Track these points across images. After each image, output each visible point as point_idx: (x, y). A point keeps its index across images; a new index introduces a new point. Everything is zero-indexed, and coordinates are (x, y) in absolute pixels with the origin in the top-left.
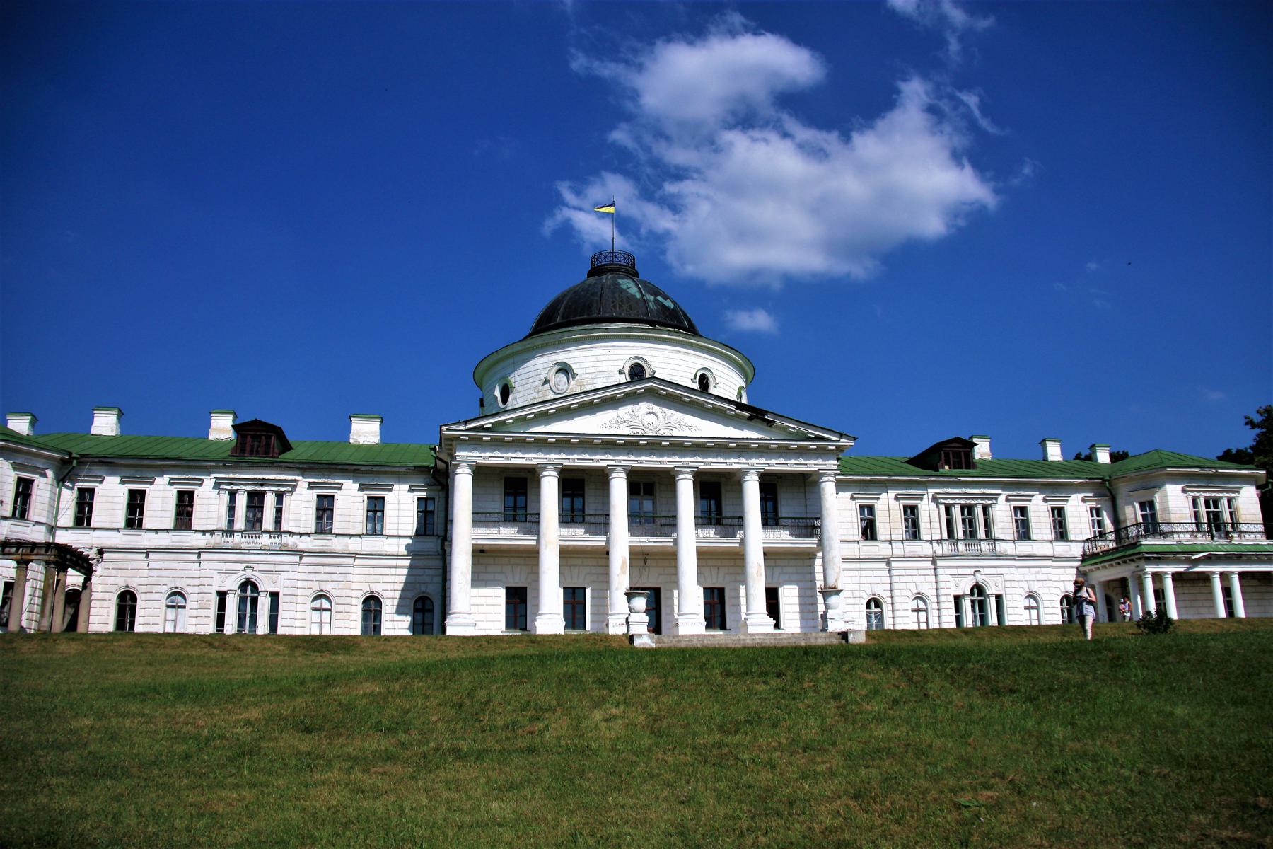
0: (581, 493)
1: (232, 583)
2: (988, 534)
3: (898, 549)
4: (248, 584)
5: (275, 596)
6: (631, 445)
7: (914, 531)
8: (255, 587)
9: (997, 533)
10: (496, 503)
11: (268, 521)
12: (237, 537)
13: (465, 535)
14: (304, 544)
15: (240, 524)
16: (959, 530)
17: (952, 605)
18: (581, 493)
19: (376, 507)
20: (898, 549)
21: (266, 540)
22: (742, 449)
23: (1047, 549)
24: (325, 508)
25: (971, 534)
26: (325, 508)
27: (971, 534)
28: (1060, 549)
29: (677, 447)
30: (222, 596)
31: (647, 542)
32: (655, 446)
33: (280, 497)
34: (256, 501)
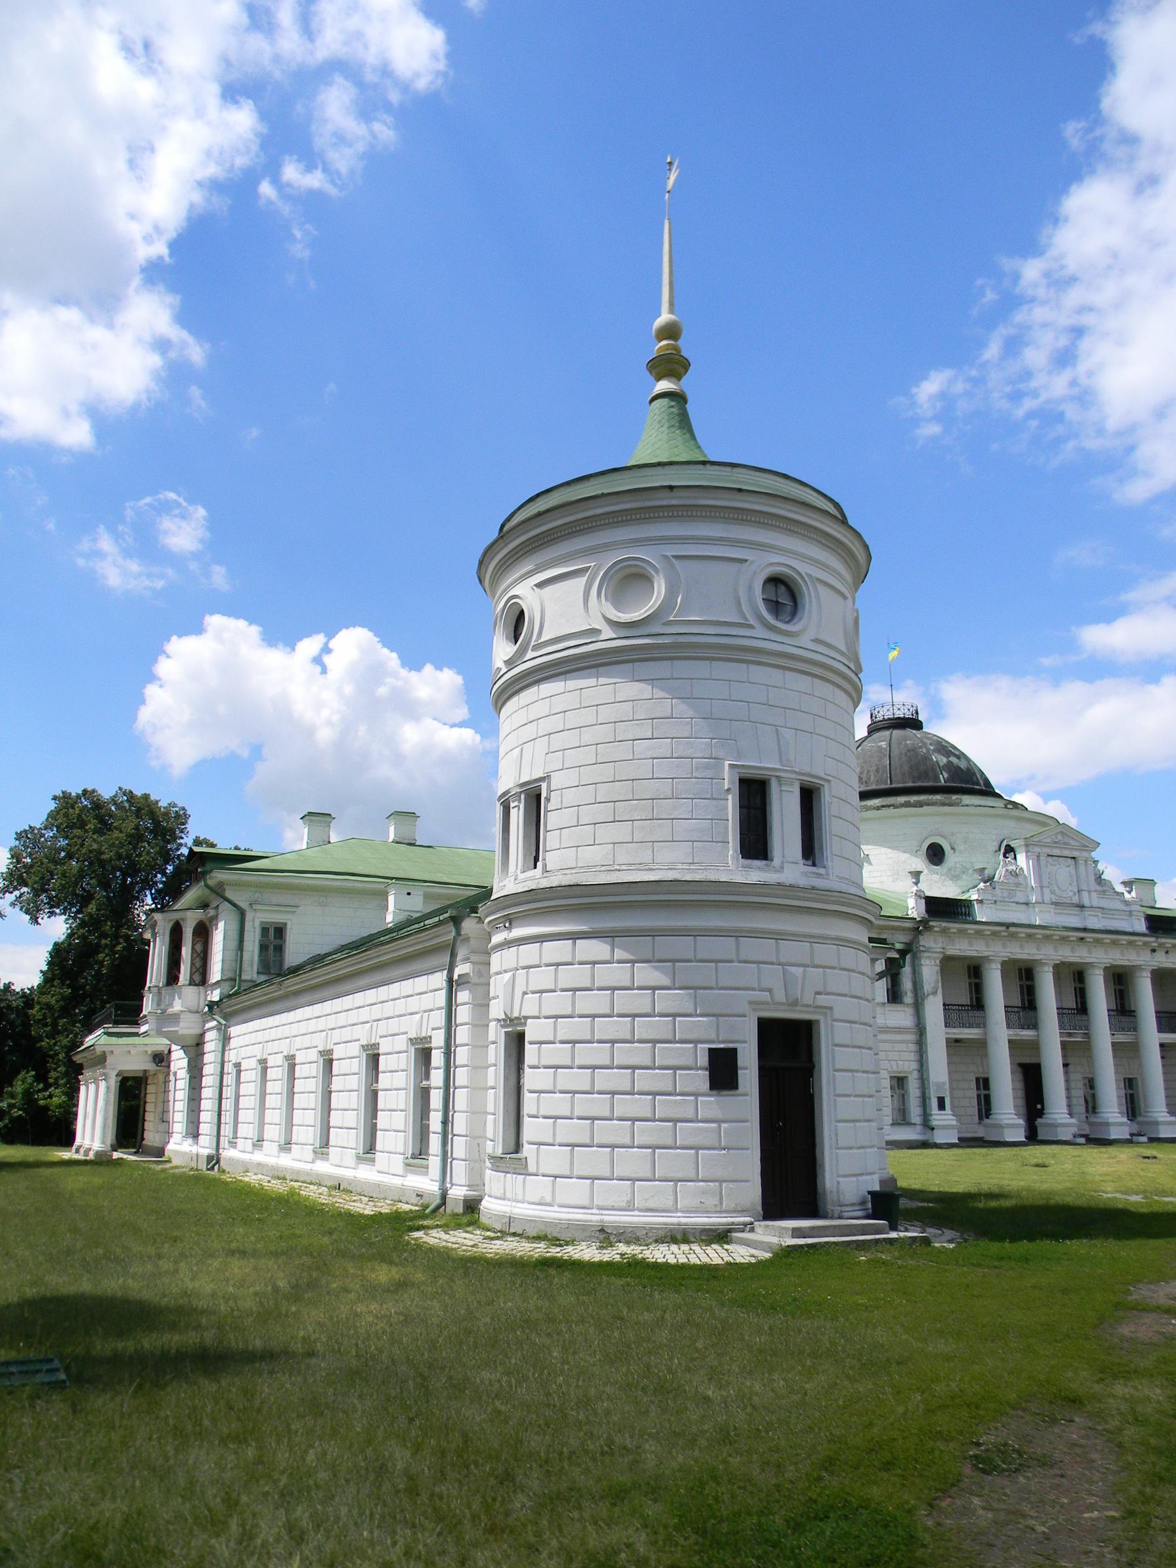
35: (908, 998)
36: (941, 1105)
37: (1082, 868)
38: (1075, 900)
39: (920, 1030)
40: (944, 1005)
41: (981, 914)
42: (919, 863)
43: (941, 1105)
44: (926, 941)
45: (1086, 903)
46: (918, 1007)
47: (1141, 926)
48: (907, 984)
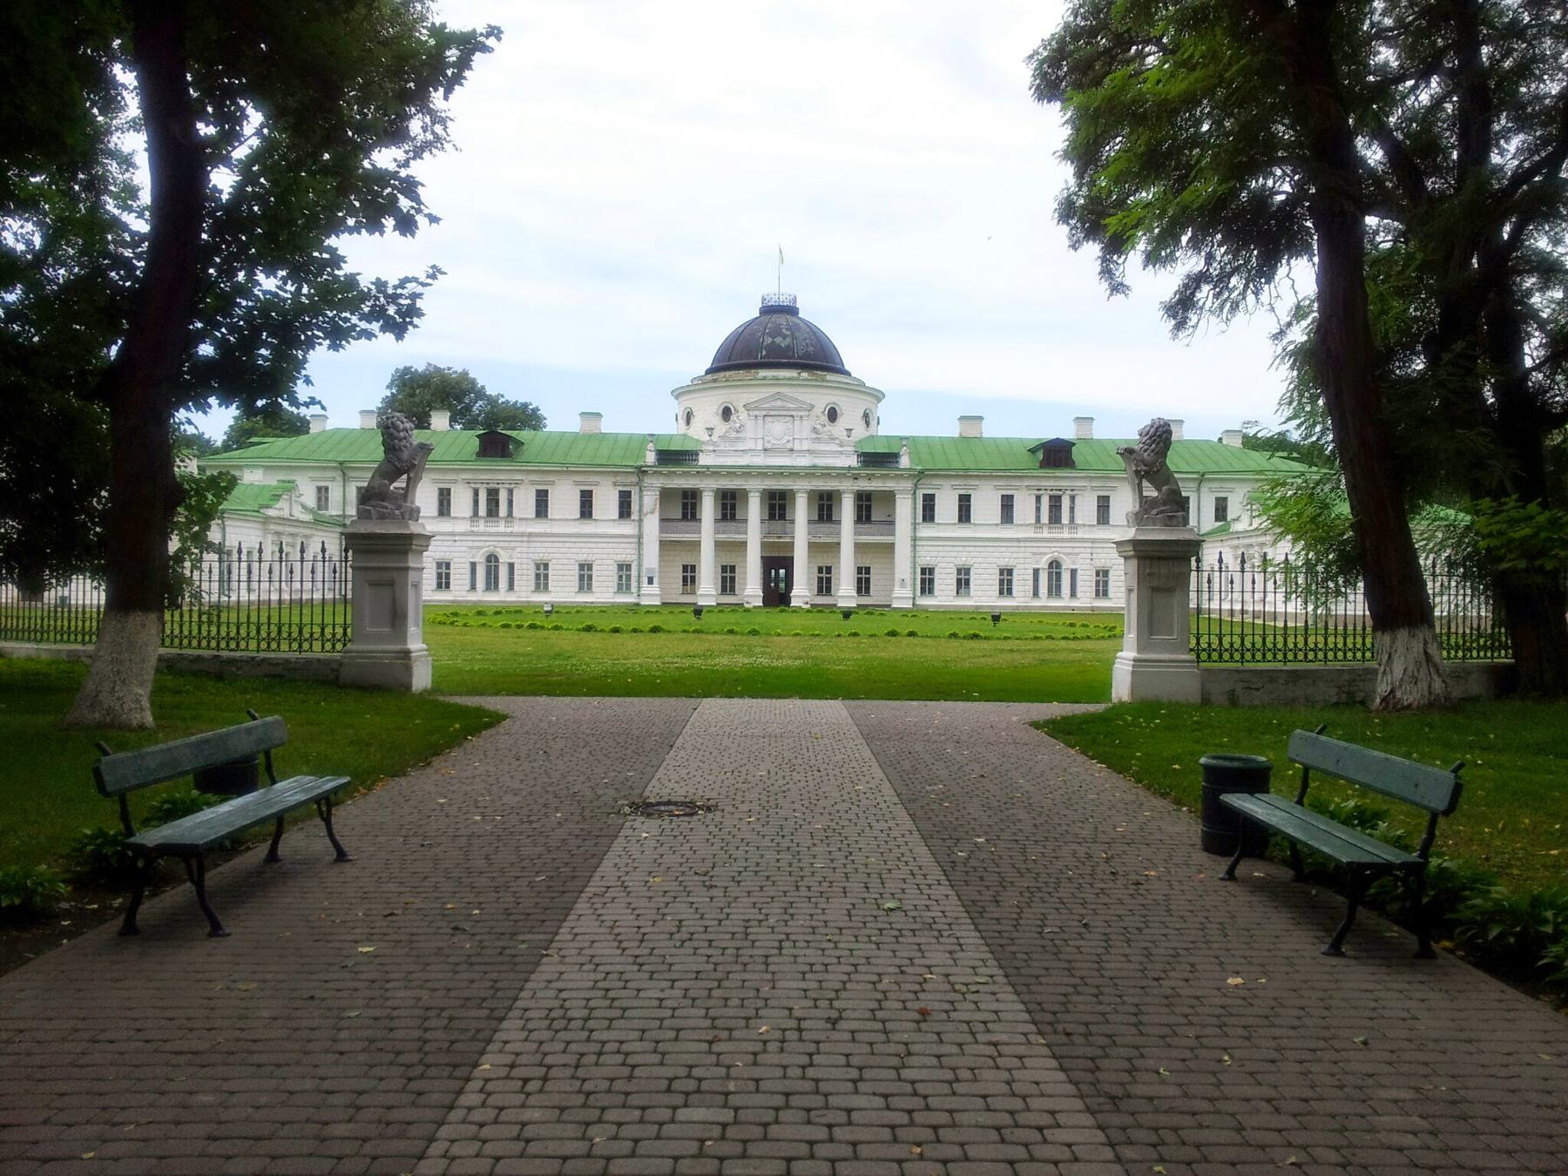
2: (1072, 519)
5: (511, 566)
8: (497, 560)
9: (1078, 521)
11: (503, 510)
12: (482, 522)
15: (482, 511)
16: (1045, 519)
17: (1031, 577)
21: (502, 523)
25: (1055, 518)
27: (1055, 518)
30: (473, 565)
33: (511, 492)
34: (493, 496)
35: (635, 516)
36: (650, 581)
37: (797, 422)
38: (789, 446)
39: (640, 537)
40: (662, 520)
41: (704, 460)
42: (716, 421)
43: (650, 581)
44: (648, 481)
45: (797, 447)
46: (641, 521)
47: (853, 461)
48: (635, 507)
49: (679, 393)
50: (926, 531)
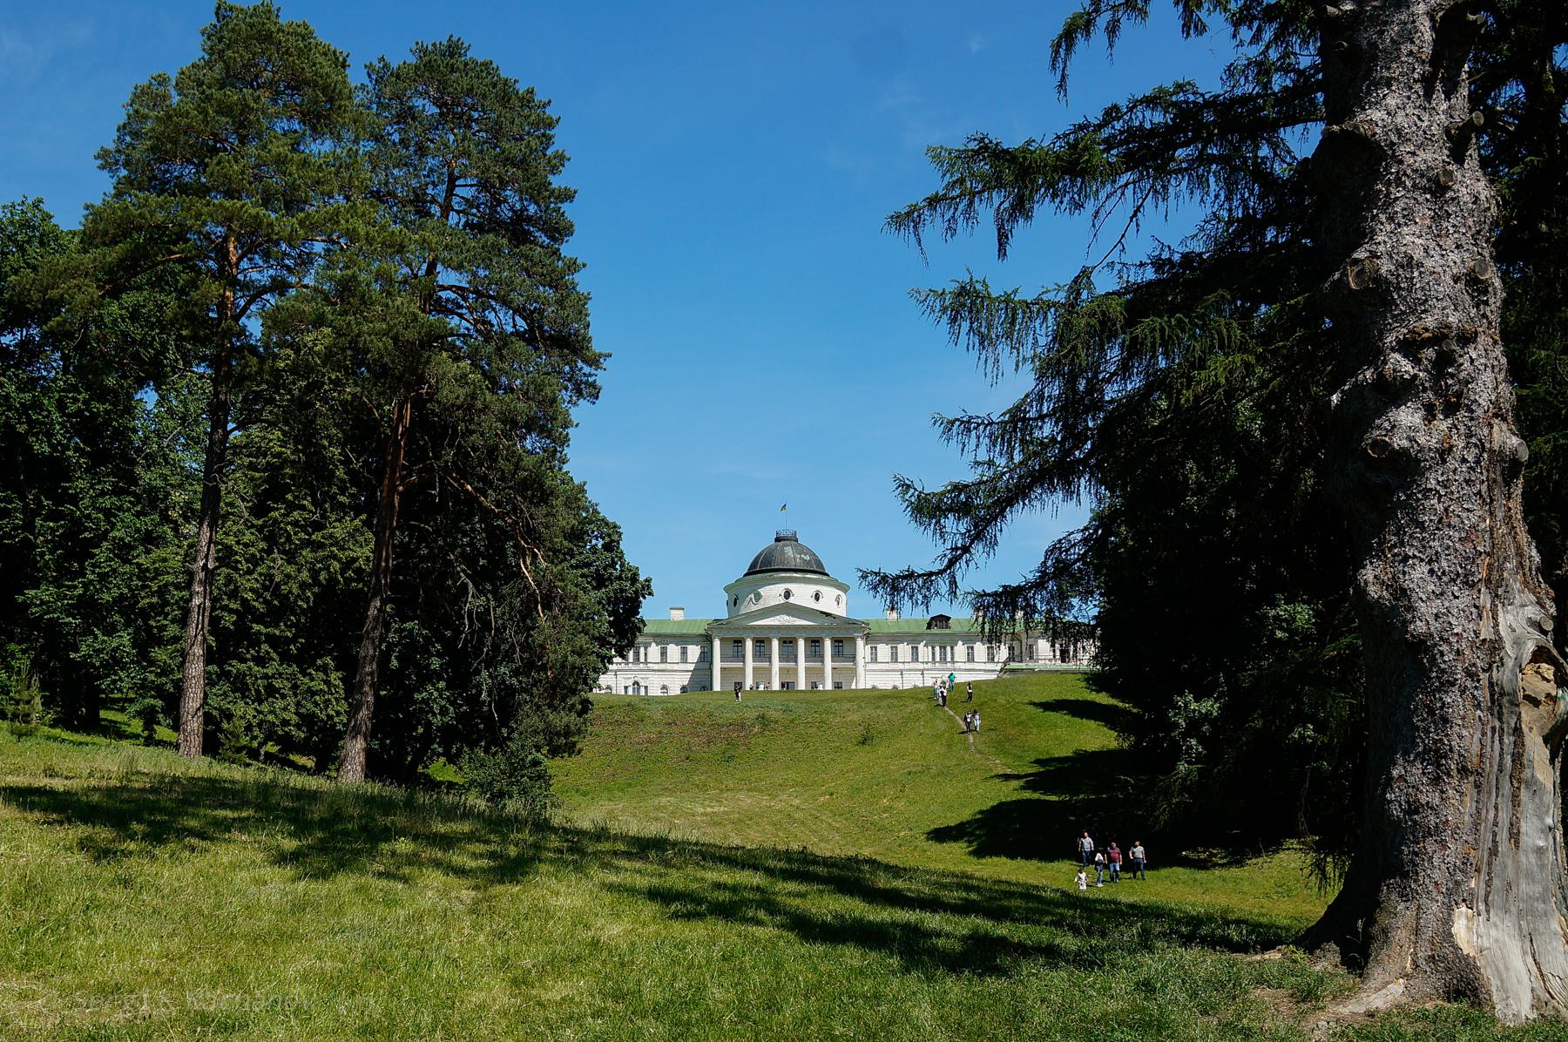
0: (761, 643)
1: (630, 683)
3: (907, 666)
4: (636, 683)
6: (778, 628)
7: (915, 659)
10: (730, 650)
13: (717, 664)
14: (656, 667)
18: (761, 643)
19: (684, 652)
20: (907, 666)
22: (822, 628)
23: (982, 666)
24: (664, 653)
26: (664, 653)
28: (991, 666)
29: (797, 628)
31: (786, 664)
32: (788, 628)
49: (727, 589)
50: (870, 666)
